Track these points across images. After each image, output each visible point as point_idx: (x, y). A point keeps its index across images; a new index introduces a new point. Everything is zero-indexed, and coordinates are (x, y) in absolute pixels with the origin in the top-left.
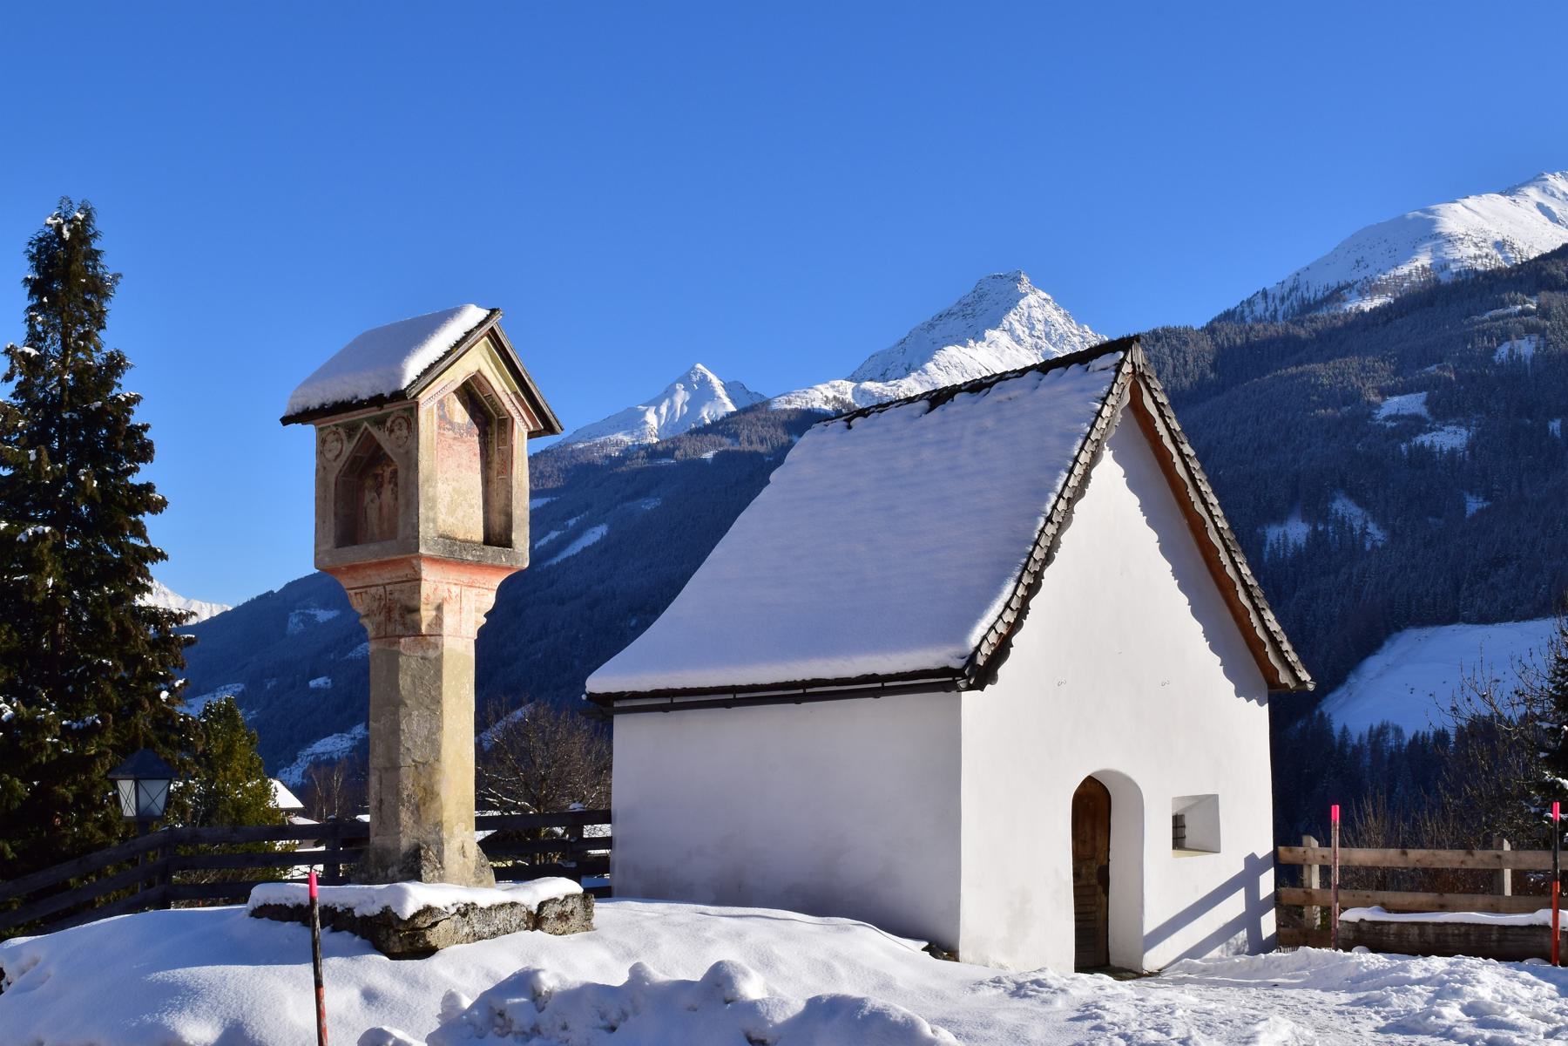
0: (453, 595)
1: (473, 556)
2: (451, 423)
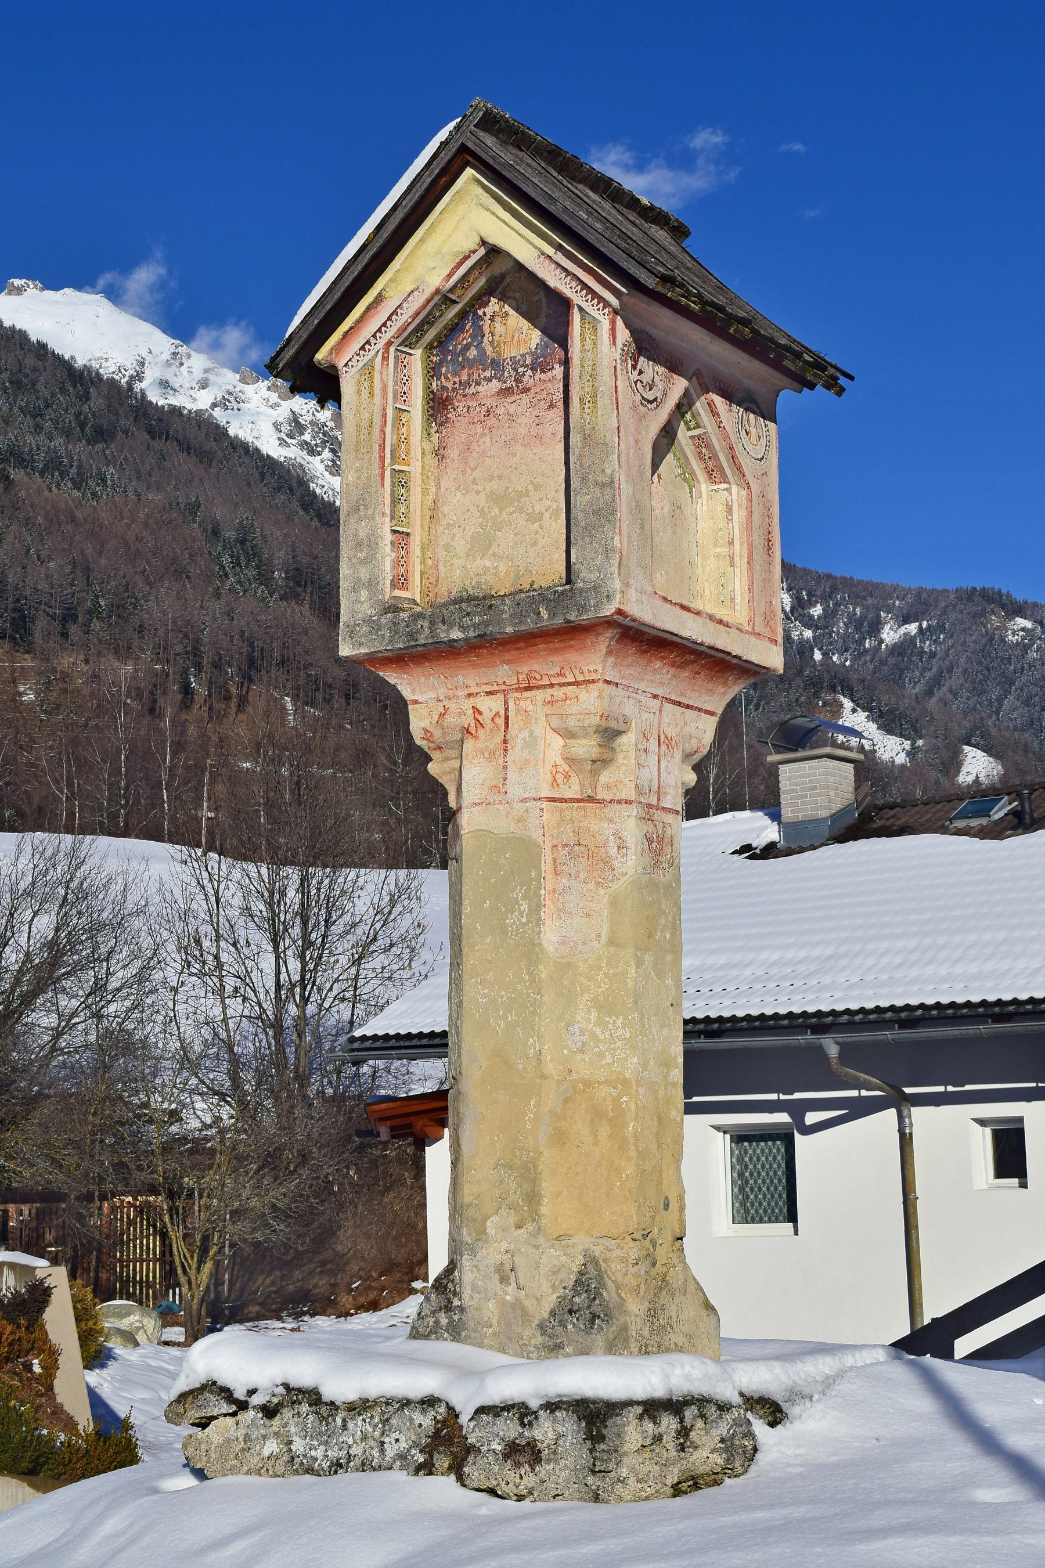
0: (486, 718)
1: (463, 628)
2: (495, 364)
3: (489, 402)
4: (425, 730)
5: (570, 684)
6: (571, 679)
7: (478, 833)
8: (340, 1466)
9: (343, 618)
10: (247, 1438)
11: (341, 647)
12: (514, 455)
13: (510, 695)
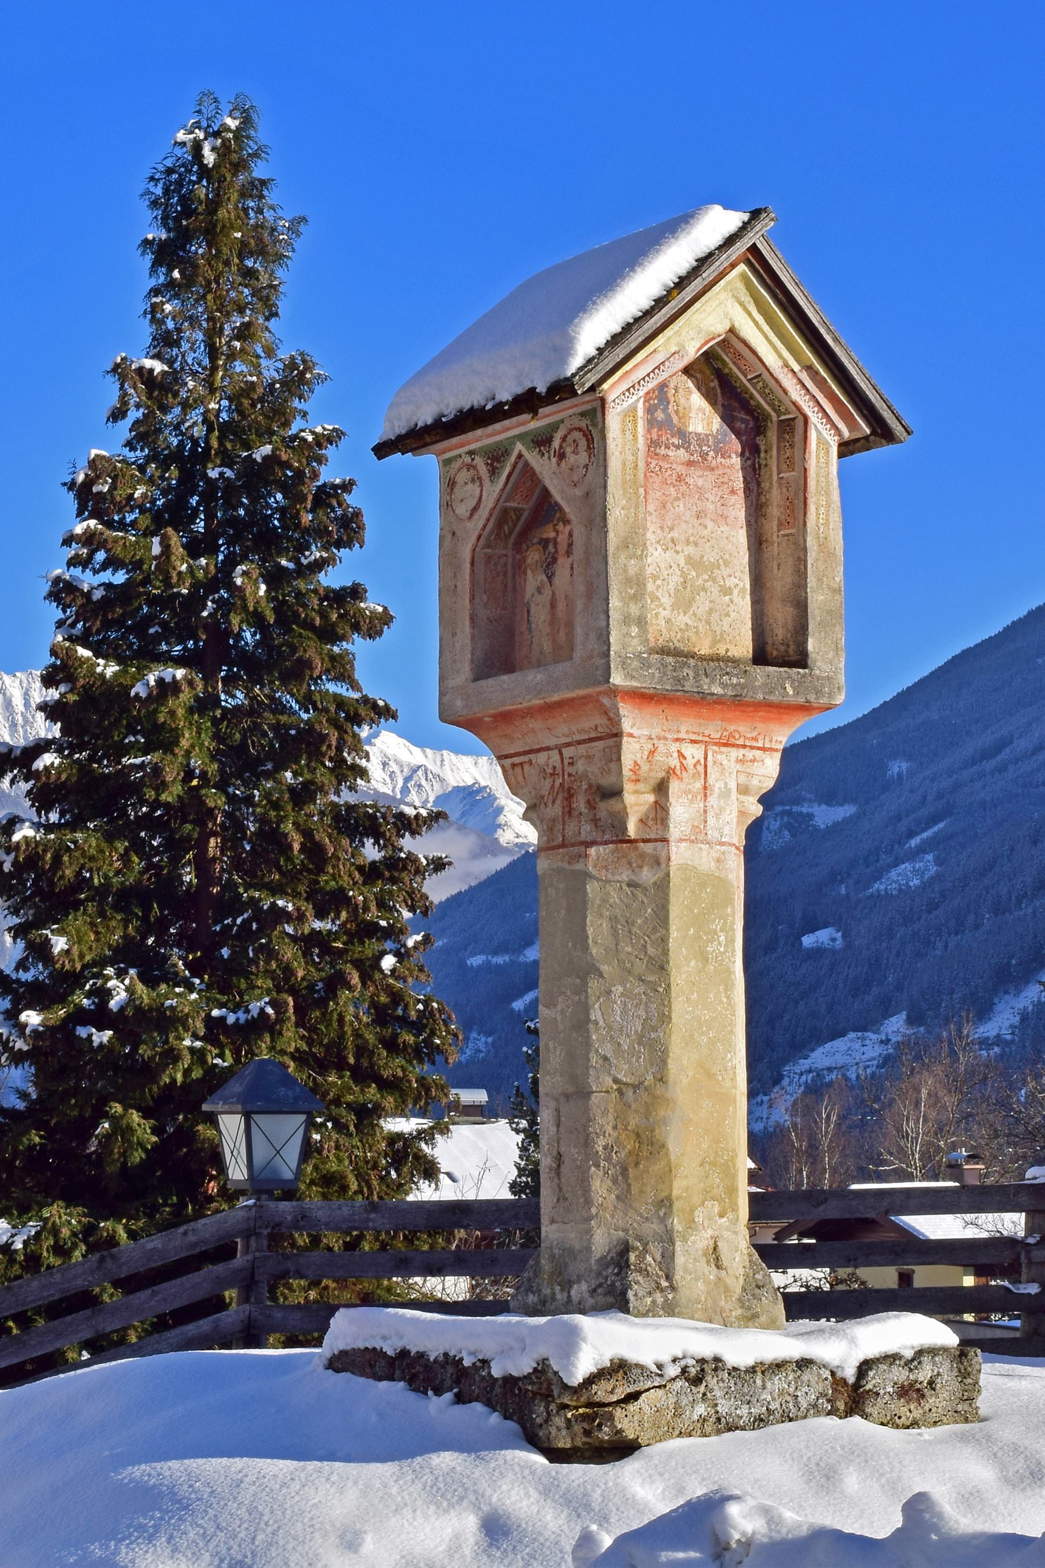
0: (690, 762)
1: (724, 686)
2: (682, 434)
3: (681, 469)
4: (636, 763)
5: (759, 748)
6: (760, 744)
7: (684, 868)
8: (762, 1420)
9: (613, 649)
10: (677, 1406)
11: (613, 675)
12: (706, 527)
13: (710, 747)
